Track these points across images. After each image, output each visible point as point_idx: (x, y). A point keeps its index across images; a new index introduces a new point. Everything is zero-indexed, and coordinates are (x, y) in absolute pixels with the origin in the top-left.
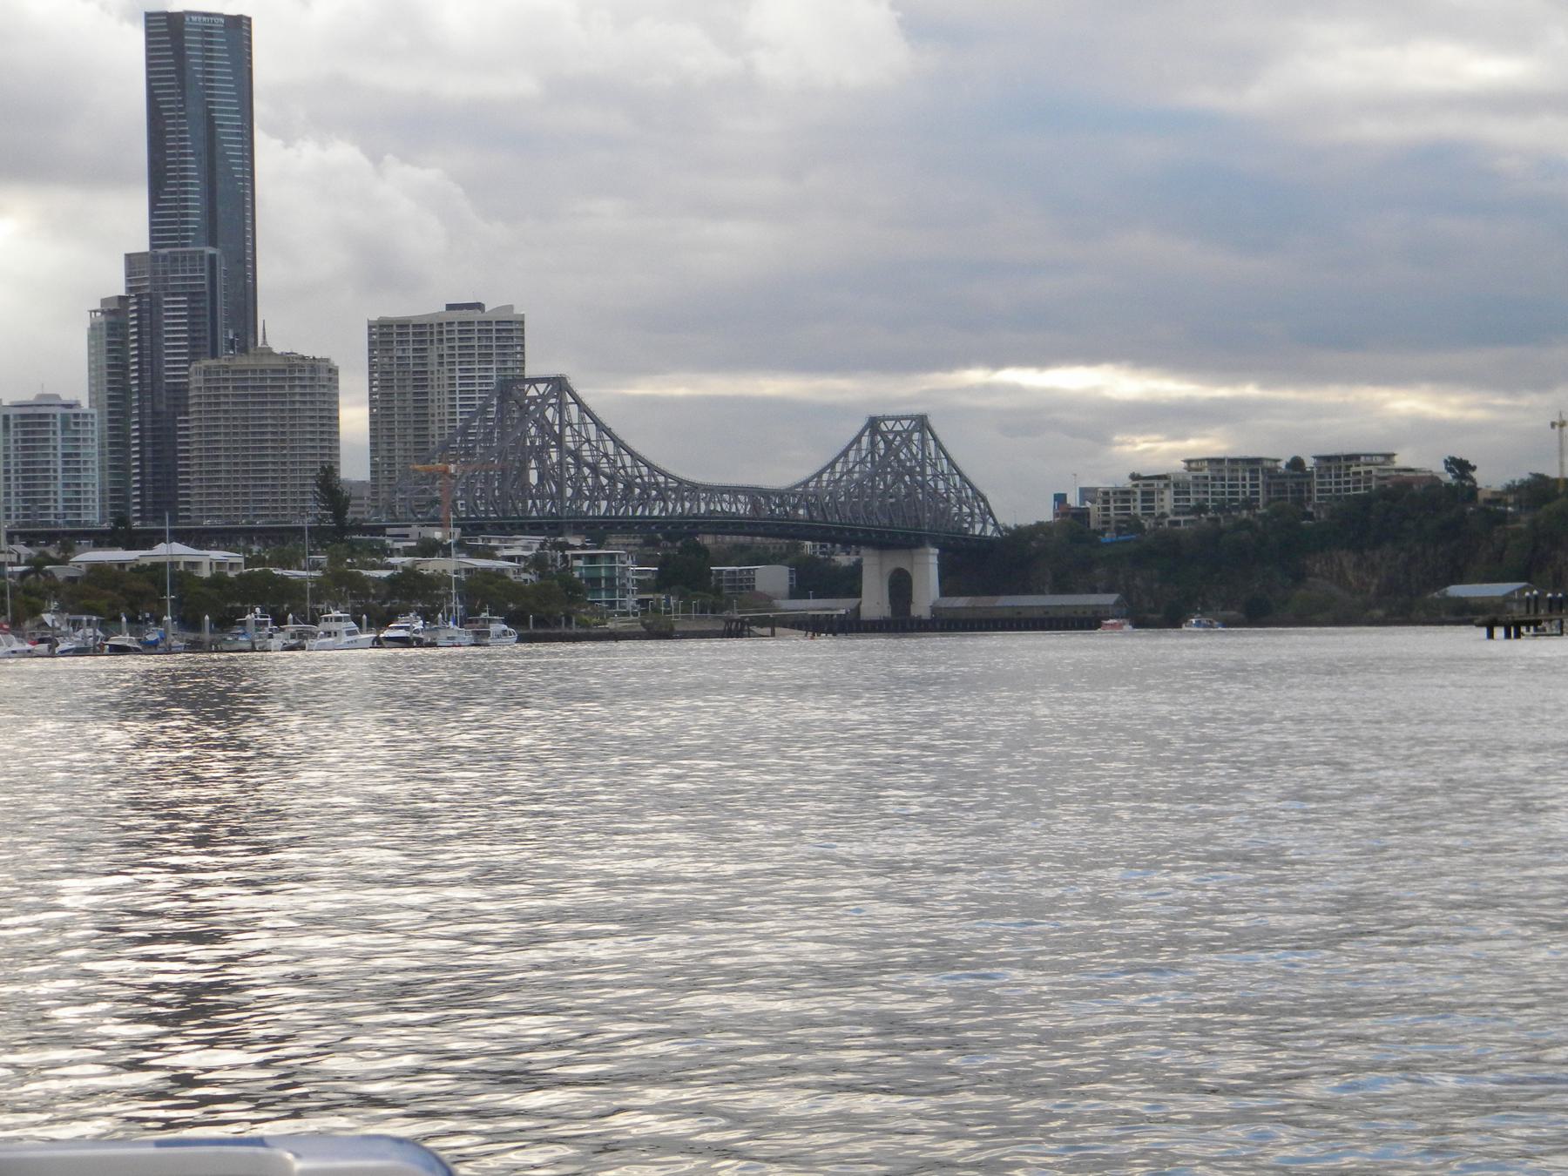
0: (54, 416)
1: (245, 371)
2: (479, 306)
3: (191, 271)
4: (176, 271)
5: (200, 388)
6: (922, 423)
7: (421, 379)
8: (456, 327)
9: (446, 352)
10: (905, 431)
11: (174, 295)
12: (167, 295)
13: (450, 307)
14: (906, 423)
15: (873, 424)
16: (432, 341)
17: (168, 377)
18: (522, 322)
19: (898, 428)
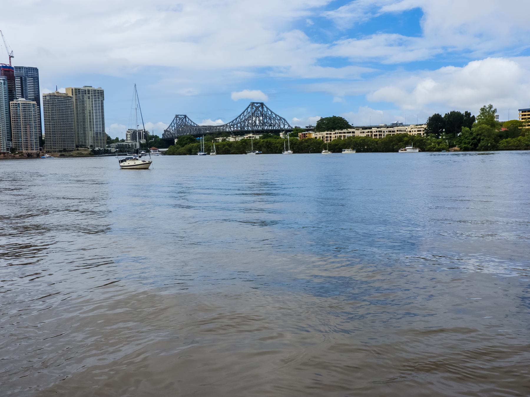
0: (31, 104)
1: (59, 97)
2: (91, 87)
3: (33, 72)
4: (30, 72)
5: (49, 100)
6: (185, 116)
7: (83, 102)
8: (93, 91)
9: (91, 96)
10: (182, 118)
11: (29, 77)
12: (28, 77)
13: (85, 86)
14: (182, 116)
15: (177, 116)
16: (86, 94)
17: (29, 97)
18: (103, 91)
19: (181, 117)
